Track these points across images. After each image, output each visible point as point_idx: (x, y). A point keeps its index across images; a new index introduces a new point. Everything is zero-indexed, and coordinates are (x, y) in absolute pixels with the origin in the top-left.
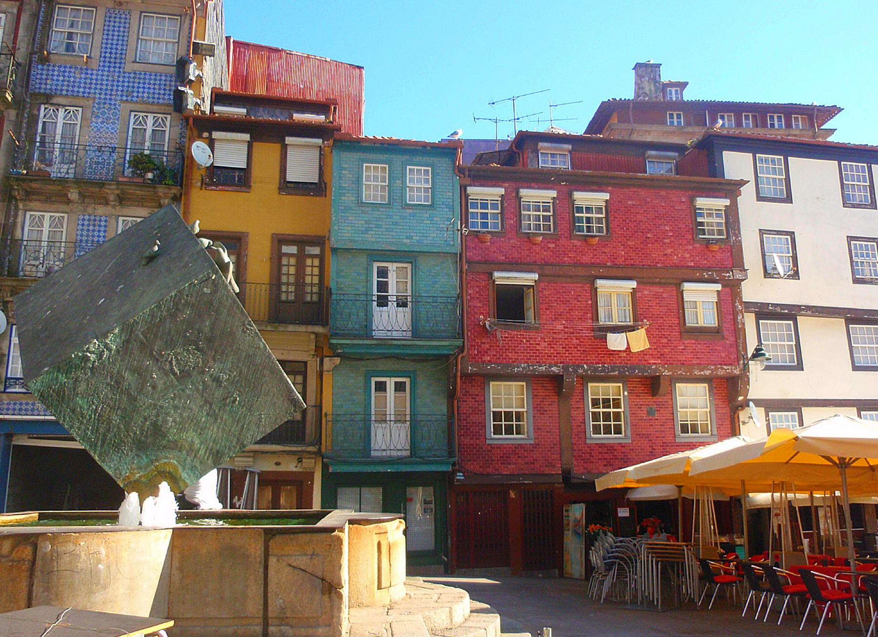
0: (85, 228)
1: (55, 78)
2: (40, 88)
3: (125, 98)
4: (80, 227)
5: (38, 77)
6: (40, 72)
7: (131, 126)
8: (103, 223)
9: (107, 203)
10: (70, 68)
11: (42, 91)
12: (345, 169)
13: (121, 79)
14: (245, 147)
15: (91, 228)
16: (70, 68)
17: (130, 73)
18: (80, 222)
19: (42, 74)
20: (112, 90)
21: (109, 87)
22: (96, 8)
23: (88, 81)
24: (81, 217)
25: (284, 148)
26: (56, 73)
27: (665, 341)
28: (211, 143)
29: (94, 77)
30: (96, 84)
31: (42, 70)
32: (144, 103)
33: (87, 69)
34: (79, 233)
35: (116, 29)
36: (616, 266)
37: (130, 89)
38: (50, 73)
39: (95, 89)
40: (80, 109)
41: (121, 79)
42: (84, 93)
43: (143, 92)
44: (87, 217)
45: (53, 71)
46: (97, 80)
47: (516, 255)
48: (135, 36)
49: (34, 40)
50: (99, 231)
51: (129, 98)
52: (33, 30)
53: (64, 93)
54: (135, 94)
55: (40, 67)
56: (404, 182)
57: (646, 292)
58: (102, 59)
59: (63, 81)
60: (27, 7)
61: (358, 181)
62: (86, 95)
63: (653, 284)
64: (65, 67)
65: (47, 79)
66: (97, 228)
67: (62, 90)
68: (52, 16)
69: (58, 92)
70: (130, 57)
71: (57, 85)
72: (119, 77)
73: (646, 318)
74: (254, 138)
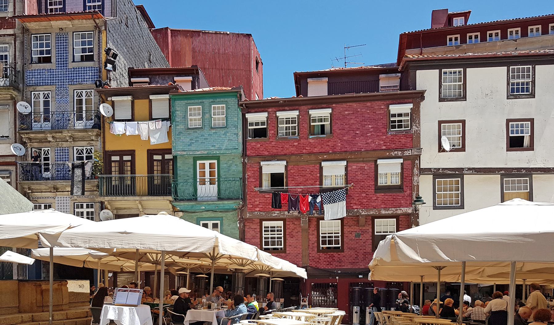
0: (59, 154)
1: (36, 77)
3: (70, 83)
4: (56, 154)
7: (75, 98)
8: (66, 151)
9: (67, 141)
10: (43, 70)
13: (67, 73)
15: (61, 154)
18: (56, 151)
20: (64, 79)
21: (62, 78)
23: (52, 76)
24: (56, 149)
25: (150, 101)
27: (364, 195)
28: (113, 104)
30: (56, 77)
32: (79, 84)
34: (56, 157)
35: (62, 44)
36: (334, 152)
37: (72, 78)
39: (56, 80)
44: (59, 149)
46: (56, 75)
47: (275, 151)
50: (65, 155)
51: (72, 83)
52: (23, 52)
53: (41, 84)
54: (75, 80)
57: (354, 167)
58: (57, 63)
59: (40, 78)
60: (18, 39)
61: (185, 117)
63: (358, 162)
66: (64, 154)
69: (39, 84)
72: (66, 72)
73: (352, 182)
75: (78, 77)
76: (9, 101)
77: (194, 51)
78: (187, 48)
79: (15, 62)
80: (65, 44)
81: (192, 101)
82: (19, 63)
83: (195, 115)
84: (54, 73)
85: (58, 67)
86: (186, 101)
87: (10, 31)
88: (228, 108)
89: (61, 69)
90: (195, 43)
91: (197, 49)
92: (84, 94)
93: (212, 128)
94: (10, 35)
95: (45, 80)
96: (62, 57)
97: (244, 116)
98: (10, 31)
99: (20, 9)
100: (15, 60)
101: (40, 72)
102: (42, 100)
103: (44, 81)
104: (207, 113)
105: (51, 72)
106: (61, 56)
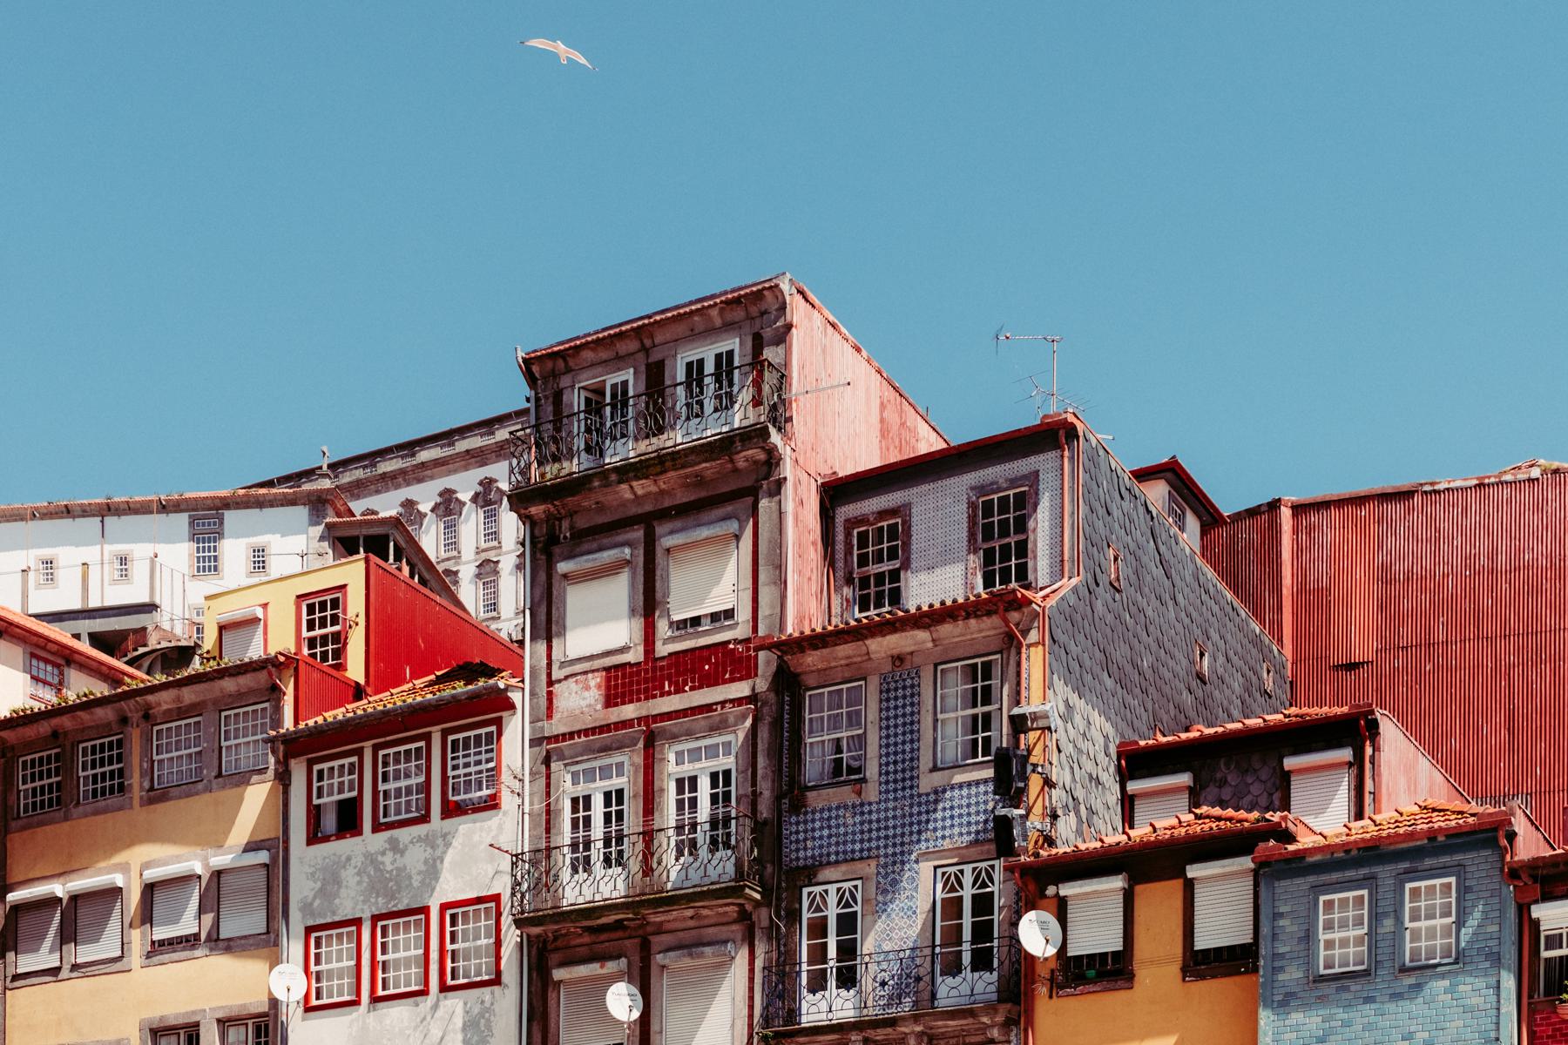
1: (817, 834)
2: (798, 859)
5: (793, 838)
6: (794, 828)
10: (838, 808)
11: (801, 863)
12: (1281, 915)
13: (915, 810)
14: (1119, 899)
16: (838, 808)
17: (927, 795)
19: (797, 832)
20: (903, 835)
21: (899, 831)
22: (865, 679)
25: (1189, 886)
26: (817, 825)
28: (1061, 910)
29: (874, 817)
30: (878, 829)
31: (798, 823)
33: (862, 805)
38: (810, 826)
39: (878, 838)
40: (859, 883)
41: (915, 810)
42: (862, 850)
43: (952, 826)
45: (813, 821)
46: (878, 821)
48: (930, 719)
49: (780, 770)
52: (775, 753)
53: (833, 858)
55: (794, 819)
56: (1399, 920)
59: (830, 836)
61: (1308, 937)
62: (865, 854)
64: (830, 810)
65: (805, 840)
67: (829, 855)
68: (801, 719)
69: (824, 859)
70: (925, 761)
71: (821, 847)
72: (911, 806)
74: (1134, 881)
75: (948, 823)
76: (734, 927)
77: (1385, 576)
78: (1359, 573)
79: (754, 792)
80: (908, 710)
81: (1335, 876)
82: (767, 794)
83: (1343, 925)
84: (874, 817)
85: (887, 792)
86: (1312, 879)
87: (741, 689)
88: (1463, 890)
89: (895, 799)
90: (1390, 542)
91: (1399, 568)
92: (968, 880)
93: (1404, 970)
94: (738, 702)
95: (845, 843)
96: (900, 757)
97: (1523, 910)
98: (741, 689)
99: (772, 607)
100: (754, 784)
101: (829, 818)
102: (832, 912)
103: (841, 848)
104: (1386, 915)
105: (862, 813)
106: (896, 753)
